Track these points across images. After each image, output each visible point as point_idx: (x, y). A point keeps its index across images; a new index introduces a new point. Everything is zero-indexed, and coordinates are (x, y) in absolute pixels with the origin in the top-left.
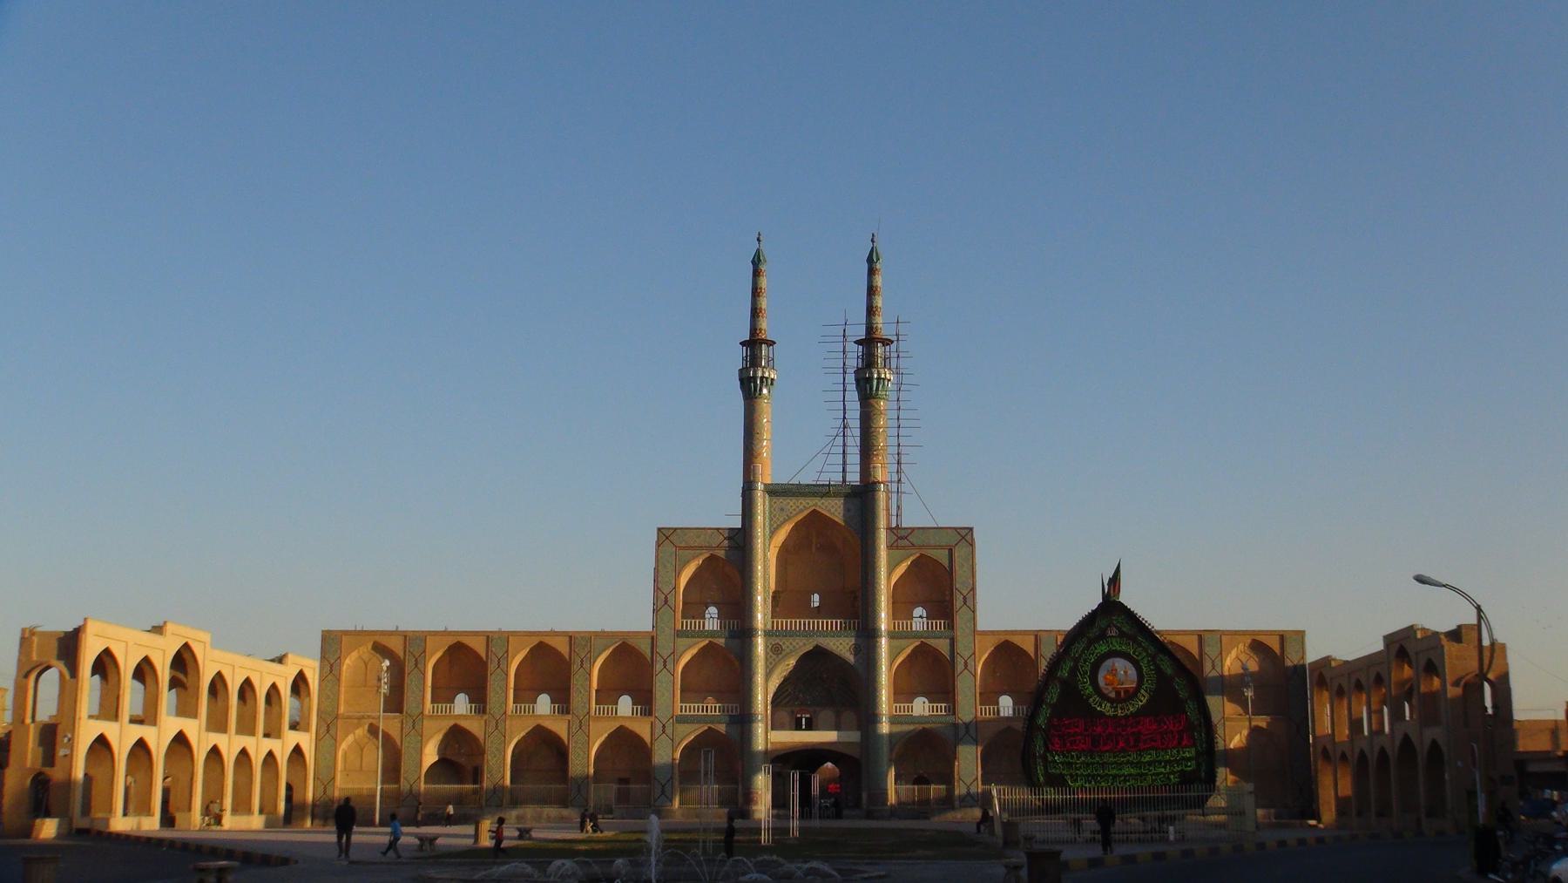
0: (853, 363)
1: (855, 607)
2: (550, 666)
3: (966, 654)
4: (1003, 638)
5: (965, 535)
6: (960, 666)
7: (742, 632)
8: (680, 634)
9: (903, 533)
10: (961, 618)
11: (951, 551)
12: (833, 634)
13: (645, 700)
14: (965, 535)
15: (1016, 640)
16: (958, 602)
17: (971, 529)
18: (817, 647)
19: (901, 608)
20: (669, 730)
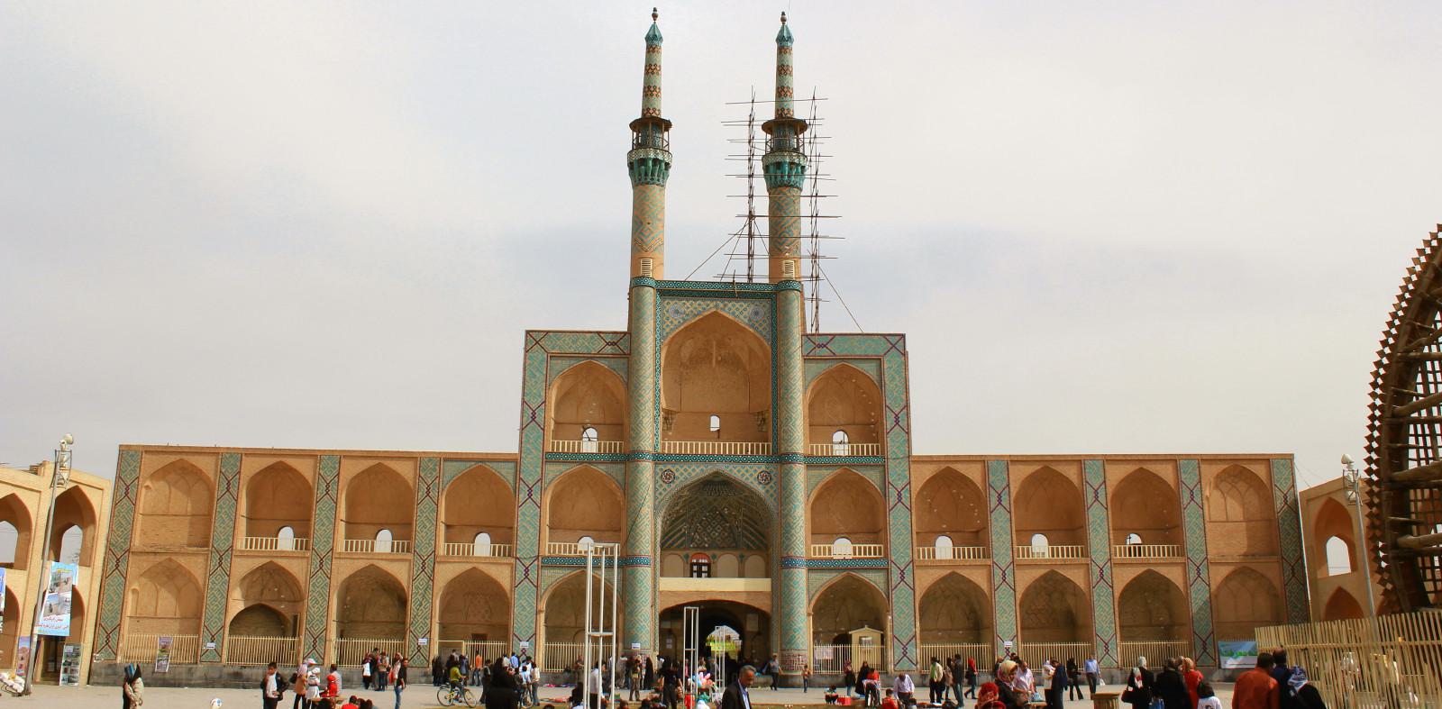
0: (761, 149)
1: (763, 426)
2: (383, 489)
3: (900, 485)
4: (943, 466)
5: (896, 343)
6: (892, 500)
7: (628, 458)
8: (550, 458)
9: (818, 340)
10: (893, 444)
11: (879, 360)
12: (743, 460)
13: (504, 535)
14: (896, 343)
15: (960, 468)
16: (889, 421)
17: (903, 336)
18: (717, 474)
19: (819, 427)
20: (533, 575)
